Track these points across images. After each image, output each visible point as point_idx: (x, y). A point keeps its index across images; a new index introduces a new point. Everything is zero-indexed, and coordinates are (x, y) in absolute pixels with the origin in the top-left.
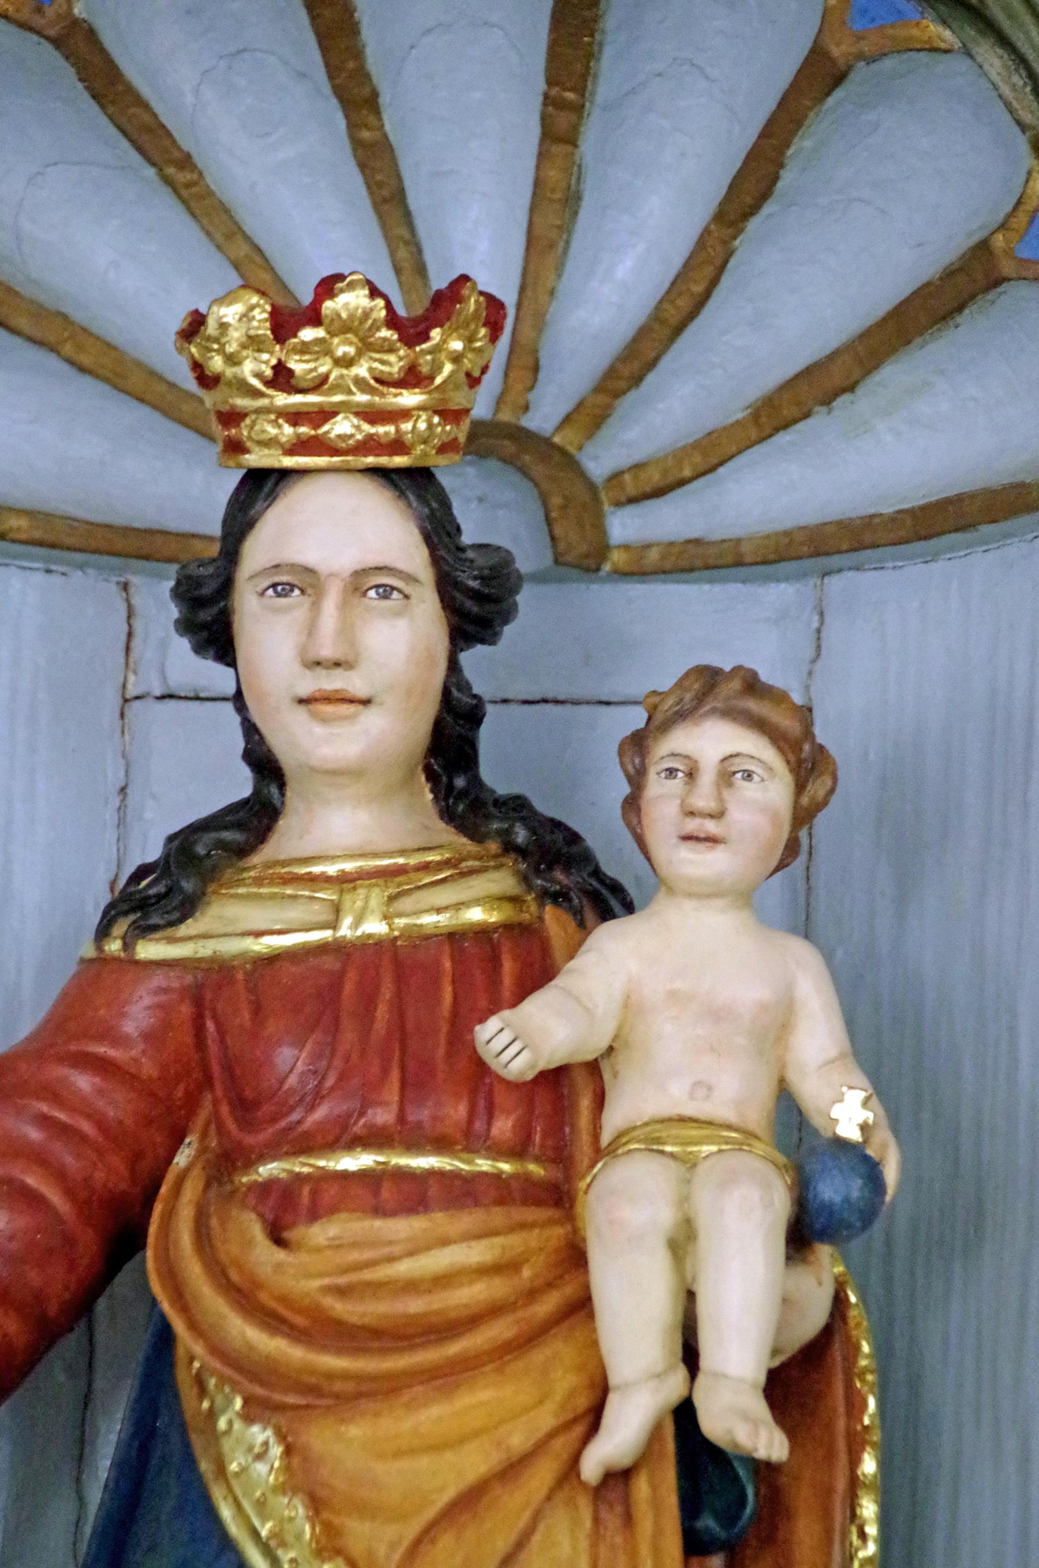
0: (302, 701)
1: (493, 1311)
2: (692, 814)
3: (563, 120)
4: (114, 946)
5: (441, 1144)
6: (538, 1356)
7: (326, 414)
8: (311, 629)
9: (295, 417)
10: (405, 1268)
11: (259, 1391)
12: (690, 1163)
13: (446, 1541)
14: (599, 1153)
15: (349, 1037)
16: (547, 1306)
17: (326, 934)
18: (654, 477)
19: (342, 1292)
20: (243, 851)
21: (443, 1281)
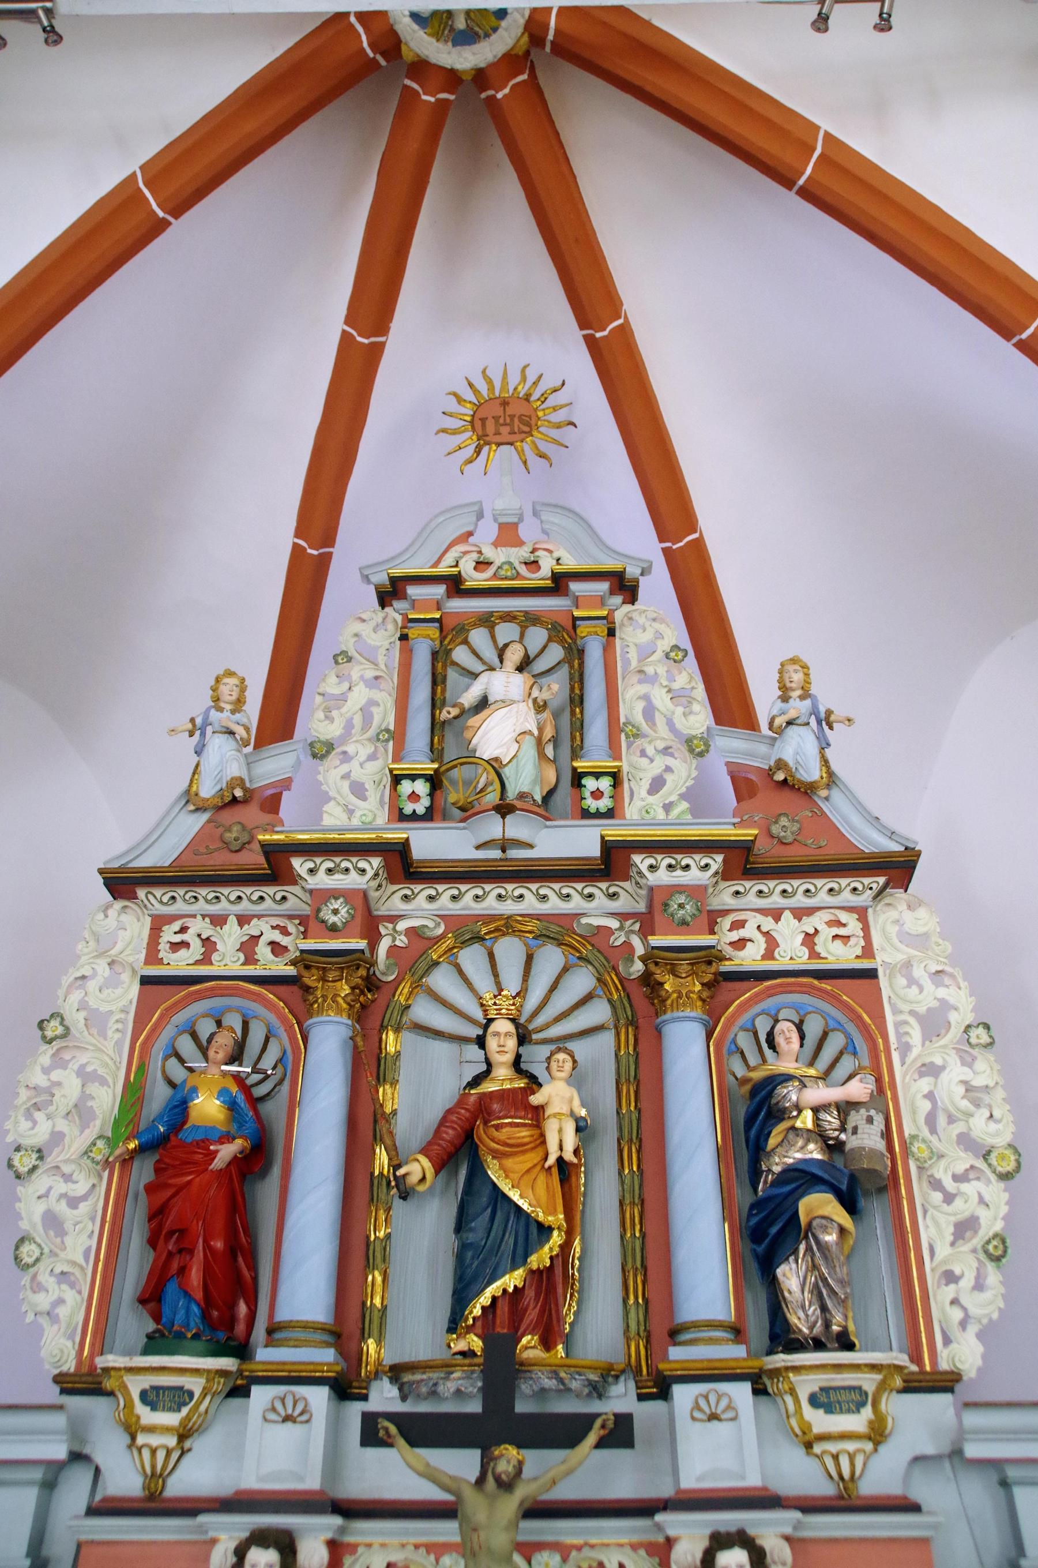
1: (530, 1142)
3: (526, 978)
4: (467, 1091)
5: (520, 1118)
6: (537, 1149)
7: (501, 1009)
8: (499, 1041)
9: (496, 1010)
10: (518, 1135)
12: (560, 1119)
13: (525, 1177)
14: (544, 1120)
15: (506, 1102)
16: (538, 1142)
18: (539, 1029)
19: (509, 1138)
20: (486, 1077)
21: (523, 1137)
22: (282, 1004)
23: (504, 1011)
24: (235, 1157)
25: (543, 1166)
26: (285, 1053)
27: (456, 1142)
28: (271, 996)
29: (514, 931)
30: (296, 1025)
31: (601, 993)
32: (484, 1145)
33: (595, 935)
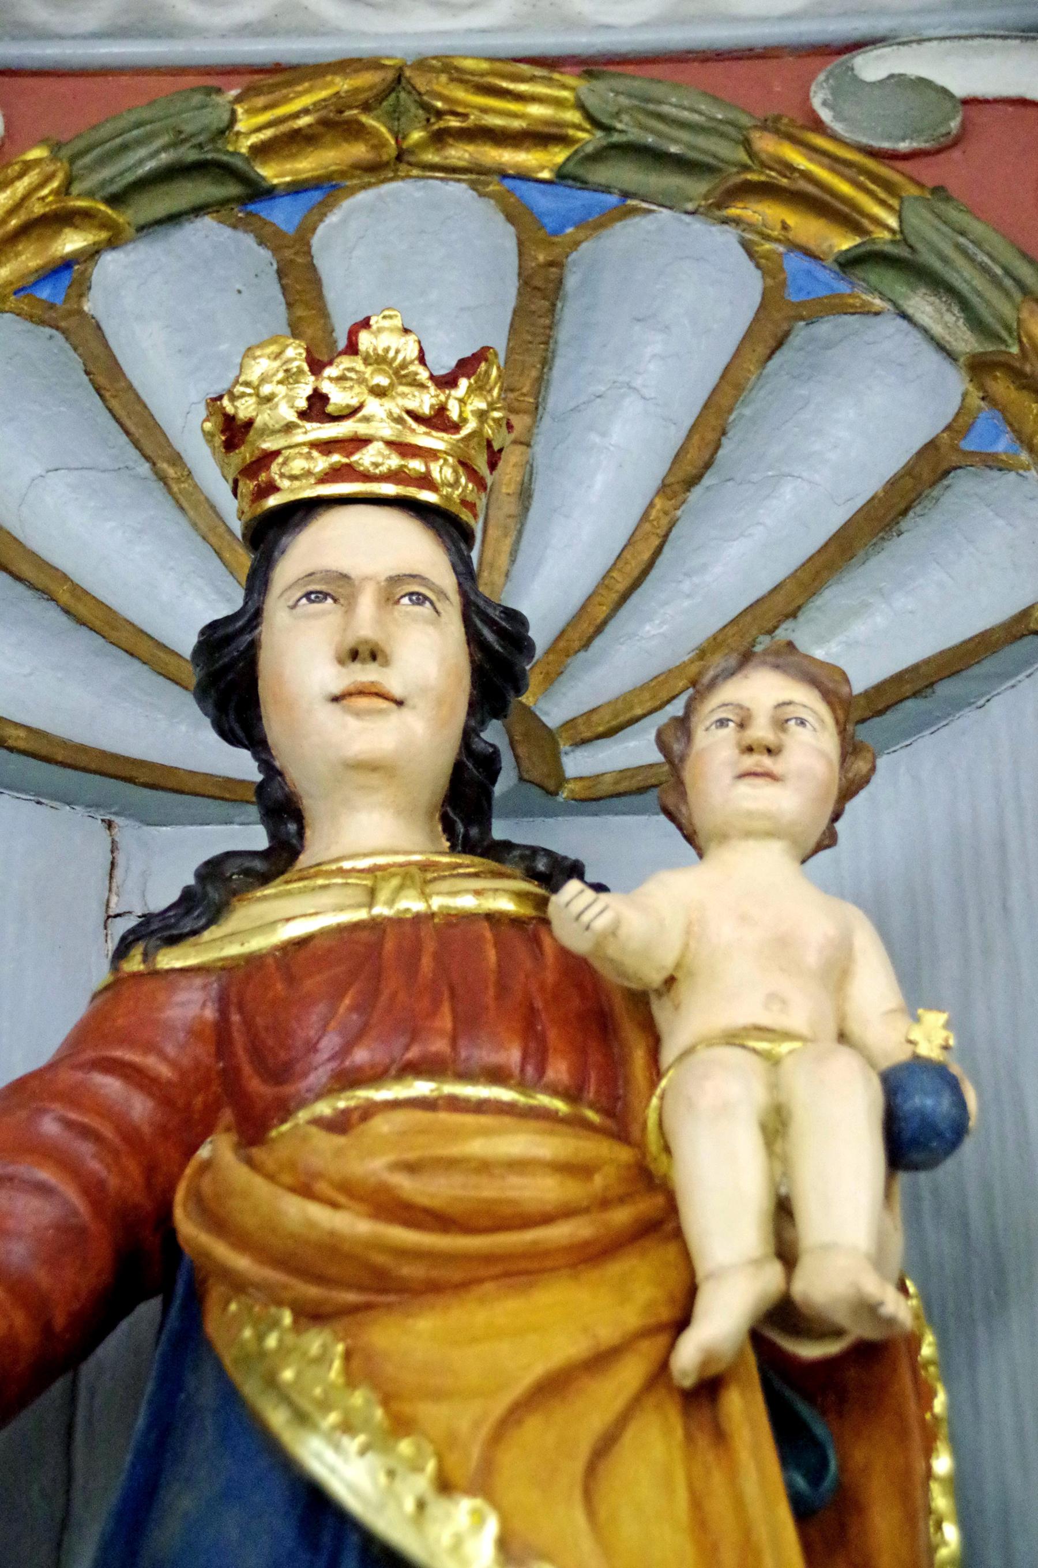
0: (336, 699)
1: (566, 1212)
2: (750, 749)
4: (134, 964)
6: (615, 1269)
7: (360, 442)
9: (326, 447)
10: (477, 1147)
11: (313, 1292)
16: (621, 1216)
17: (362, 915)
19: (412, 1168)
21: (519, 1166)
23: (366, 458)
25: (663, 1368)
27: (42, 1277)
29: (440, 138)
31: (1003, 444)
32: (242, 1242)
33: (956, 142)
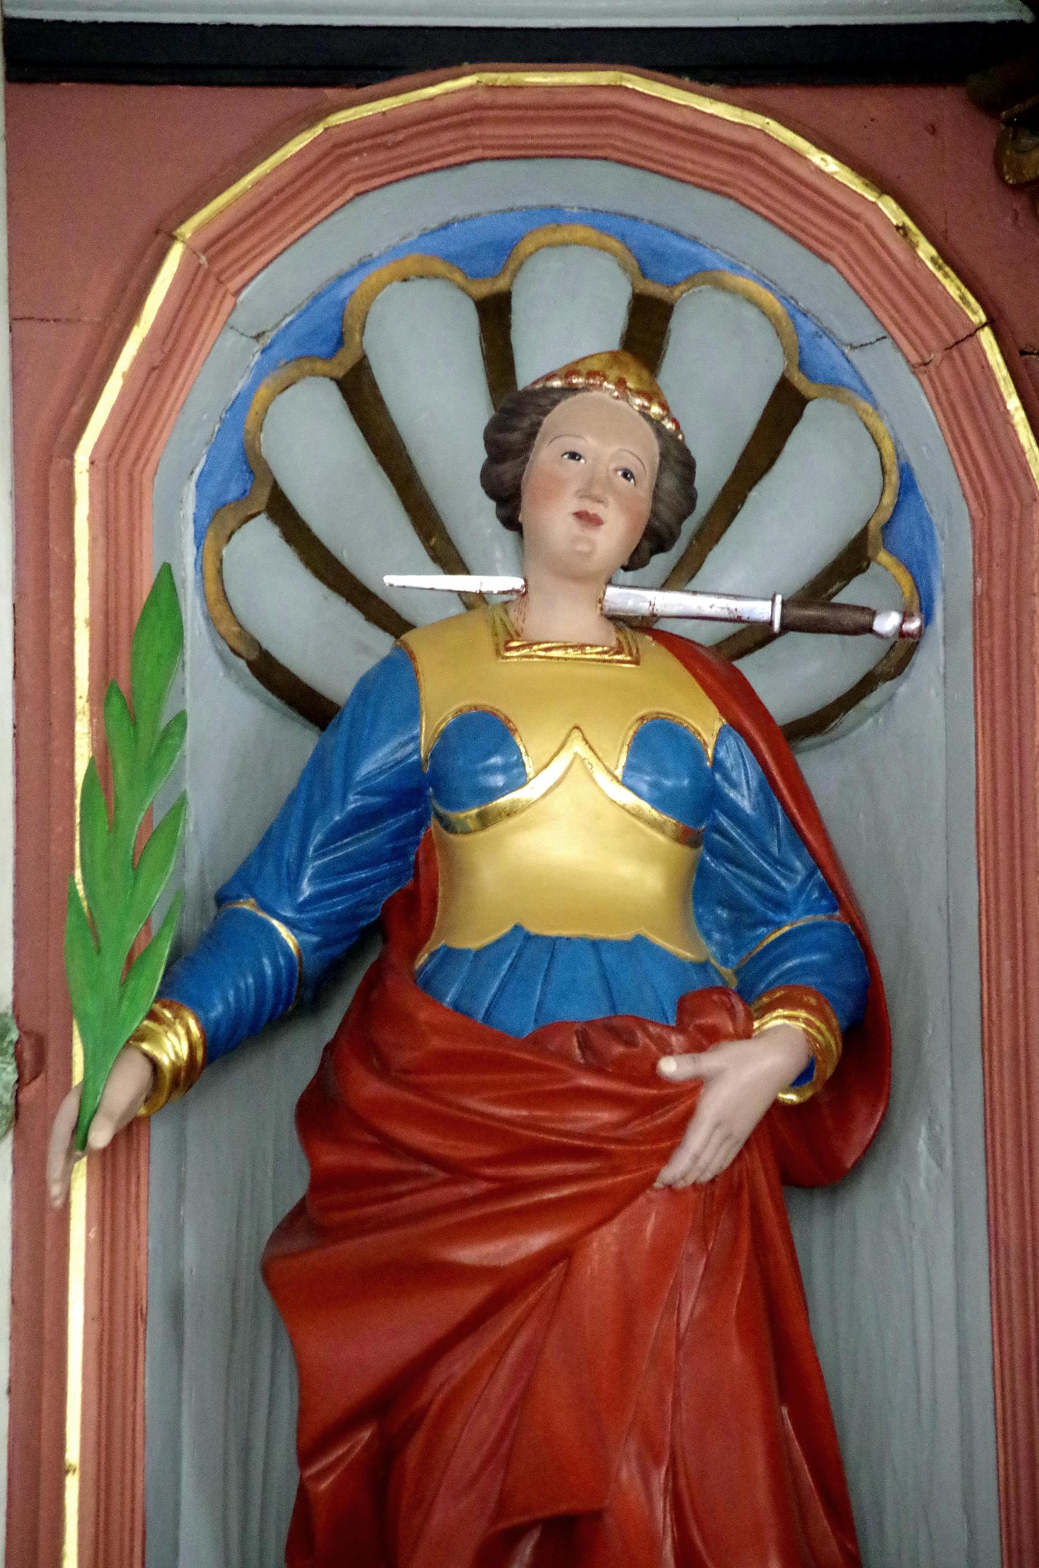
22: (891, 210)
24: (777, 1110)
26: (907, 485)
28: (831, 165)
30: (987, 337)
